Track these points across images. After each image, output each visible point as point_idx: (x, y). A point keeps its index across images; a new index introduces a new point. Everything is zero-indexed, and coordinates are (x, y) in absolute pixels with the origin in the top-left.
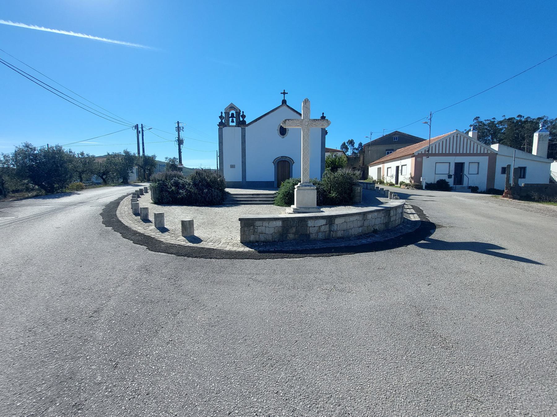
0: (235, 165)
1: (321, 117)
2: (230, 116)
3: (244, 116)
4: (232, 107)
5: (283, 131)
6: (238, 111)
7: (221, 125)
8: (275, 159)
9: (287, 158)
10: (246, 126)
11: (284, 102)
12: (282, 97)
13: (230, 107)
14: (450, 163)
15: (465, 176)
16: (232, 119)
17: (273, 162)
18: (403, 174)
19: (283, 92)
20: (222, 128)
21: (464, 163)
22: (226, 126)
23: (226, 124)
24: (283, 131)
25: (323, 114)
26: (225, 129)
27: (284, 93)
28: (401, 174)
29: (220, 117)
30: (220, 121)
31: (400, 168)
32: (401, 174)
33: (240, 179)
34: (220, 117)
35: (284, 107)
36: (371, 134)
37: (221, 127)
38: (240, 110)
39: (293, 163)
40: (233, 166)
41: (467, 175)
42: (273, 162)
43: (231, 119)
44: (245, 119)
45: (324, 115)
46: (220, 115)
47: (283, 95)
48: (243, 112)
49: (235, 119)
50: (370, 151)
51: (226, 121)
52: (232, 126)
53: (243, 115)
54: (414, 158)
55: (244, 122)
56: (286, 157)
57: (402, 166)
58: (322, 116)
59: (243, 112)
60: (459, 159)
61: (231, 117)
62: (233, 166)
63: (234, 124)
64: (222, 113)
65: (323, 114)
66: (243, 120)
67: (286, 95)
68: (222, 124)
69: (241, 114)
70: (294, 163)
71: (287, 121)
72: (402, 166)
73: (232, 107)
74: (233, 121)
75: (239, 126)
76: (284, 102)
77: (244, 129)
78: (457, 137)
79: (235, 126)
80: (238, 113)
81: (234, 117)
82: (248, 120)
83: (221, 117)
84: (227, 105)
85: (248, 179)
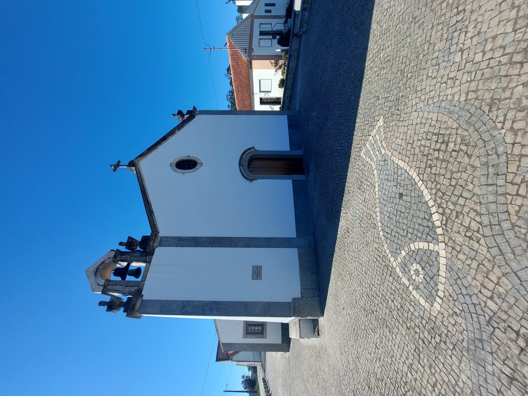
0: (253, 267)
2: (119, 279)
3: (130, 243)
6: (114, 253)
10: (156, 235)
11: (132, 164)
13: (96, 274)
14: (260, 39)
15: (273, 30)
16: (128, 275)
18: (270, 90)
21: (260, 31)
23: (133, 289)
25: (174, 115)
26: (147, 294)
28: (270, 92)
31: (263, 95)
32: (270, 92)
35: (144, 164)
37: (138, 304)
38: (112, 251)
39: (254, 150)
40: (257, 273)
41: (273, 27)
43: (129, 278)
44: (139, 239)
48: (121, 244)
54: (252, 61)
55: (146, 240)
56: (241, 159)
57: (260, 92)
59: (121, 244)
60: (256, 32)
61: (124, 278)
62: (257, 273)
63: (142, 265)
64: (101, 304)
69: (123, 249)
70: (253, 148)
72: (260, 92)
76: (132, 164)
78: (233, 35)
79: (149, 262)
80: (118, 255)
81: (128, 265)
83: (111, 306)
85: (291, 232)
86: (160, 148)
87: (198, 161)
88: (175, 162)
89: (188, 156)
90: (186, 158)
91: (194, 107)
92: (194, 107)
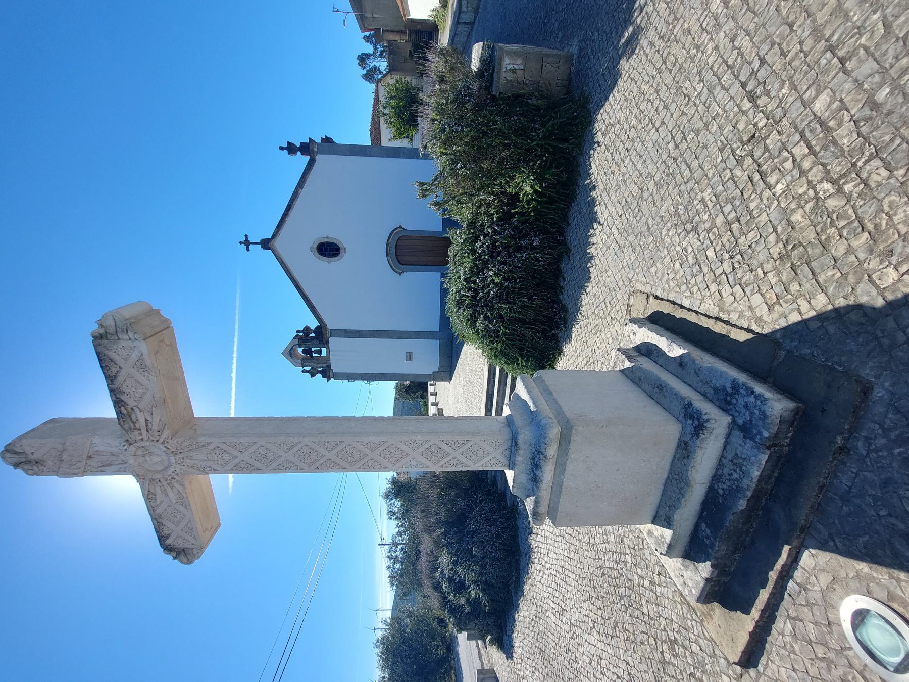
1: (289, 153)
4: (290, 353)
5: (329, 250)
6: (297, 341)
7: (327, 373)
8: (393, 269)
9: (390, 242)
11: (266, 244)
12: (256, 249)
17: (400, 274)
19: (244, 247)
20: (333, 373)
22: (329, 367)
23: (324, 365)
24: (329, 250)
25: (281, 148)
26: (336, 368)
27: (247, 243)
29: (313, 375)
30: (319, 376)
33: (434, 345)
34: (313, 375)
35: (278, 244)
36: (338, 11)
37: (331, 374)
38: (294, 339)
39: (401, 230)
40: (409, 357)
42: (400, 274)
45: (285, 145)
46: (308, 375)
47: (251, 247)
49: (313, 349)
50: (375, 15)
51: (319, 366)
52: (328, 353)
53: (303, 332)
56: (388, 244)
58: (286, 151)
59: (298, 332)
62: (409, 357)
64: (304, 372)
65: (281, 148)
66: (314, 332)
67: (251, 240)
68: (325, 372)
70: (401, 227)
71: (168, 542)
73: (290, 353)
74: (320, 352)
75: (328, 342)
76: (266, 244)
77: (333, 331)
79: (328, 348)
82: (314, 324)
84: (287, 363)
85: (436, 328)
86: (289, 220)
87: (340, 246)
88: (315, 246)
89: (327, 237)
90: (326, 240)
91: (309, 138)
92: (309, 138)
